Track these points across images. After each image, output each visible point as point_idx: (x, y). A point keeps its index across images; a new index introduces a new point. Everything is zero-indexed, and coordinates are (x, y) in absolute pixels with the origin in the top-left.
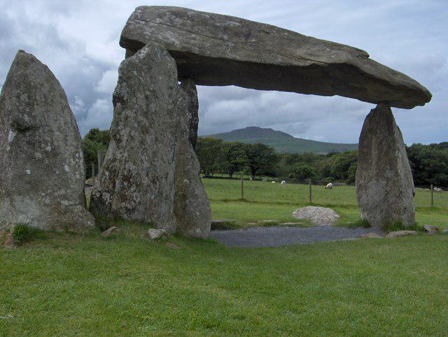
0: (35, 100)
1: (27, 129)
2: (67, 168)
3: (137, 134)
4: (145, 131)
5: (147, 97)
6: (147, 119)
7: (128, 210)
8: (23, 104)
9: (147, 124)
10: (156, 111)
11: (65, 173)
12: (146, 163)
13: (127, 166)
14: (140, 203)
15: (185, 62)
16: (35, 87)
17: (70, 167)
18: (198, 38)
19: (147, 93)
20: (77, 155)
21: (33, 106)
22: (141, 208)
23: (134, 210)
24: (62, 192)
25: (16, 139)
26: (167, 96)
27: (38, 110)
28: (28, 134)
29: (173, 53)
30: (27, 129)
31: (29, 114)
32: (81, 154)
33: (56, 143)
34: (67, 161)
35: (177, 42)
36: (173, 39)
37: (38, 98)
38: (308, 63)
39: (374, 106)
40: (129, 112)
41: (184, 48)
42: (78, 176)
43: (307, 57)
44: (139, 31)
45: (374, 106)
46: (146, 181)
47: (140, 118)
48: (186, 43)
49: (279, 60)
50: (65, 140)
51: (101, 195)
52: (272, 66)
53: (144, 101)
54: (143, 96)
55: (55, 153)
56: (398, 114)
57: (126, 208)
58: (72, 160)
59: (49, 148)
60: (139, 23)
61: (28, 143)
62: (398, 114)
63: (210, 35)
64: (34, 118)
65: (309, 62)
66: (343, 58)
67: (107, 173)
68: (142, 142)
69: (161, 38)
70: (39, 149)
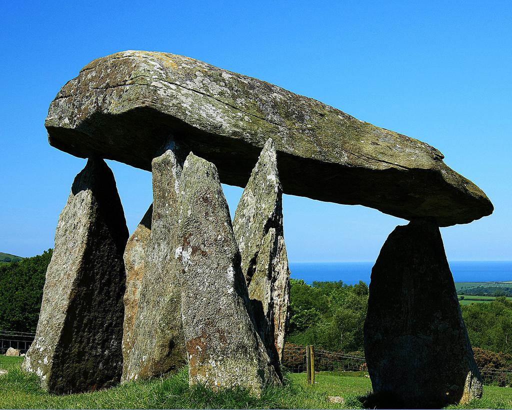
15: (218, 151)
18: (246, 118)
35: (225, 125)
36: (218, 119)
38: (383, 166)
39: (405, 222)
41: (235, 133)
43: (380, 157)
44: (175, 101)
45: (405, 222)
48: (236, 126)
49: (344, 159)
52: (336, 166)
63: (259, 115)
65: (386, 164)
66: (426, 163)
69: (205, 116)
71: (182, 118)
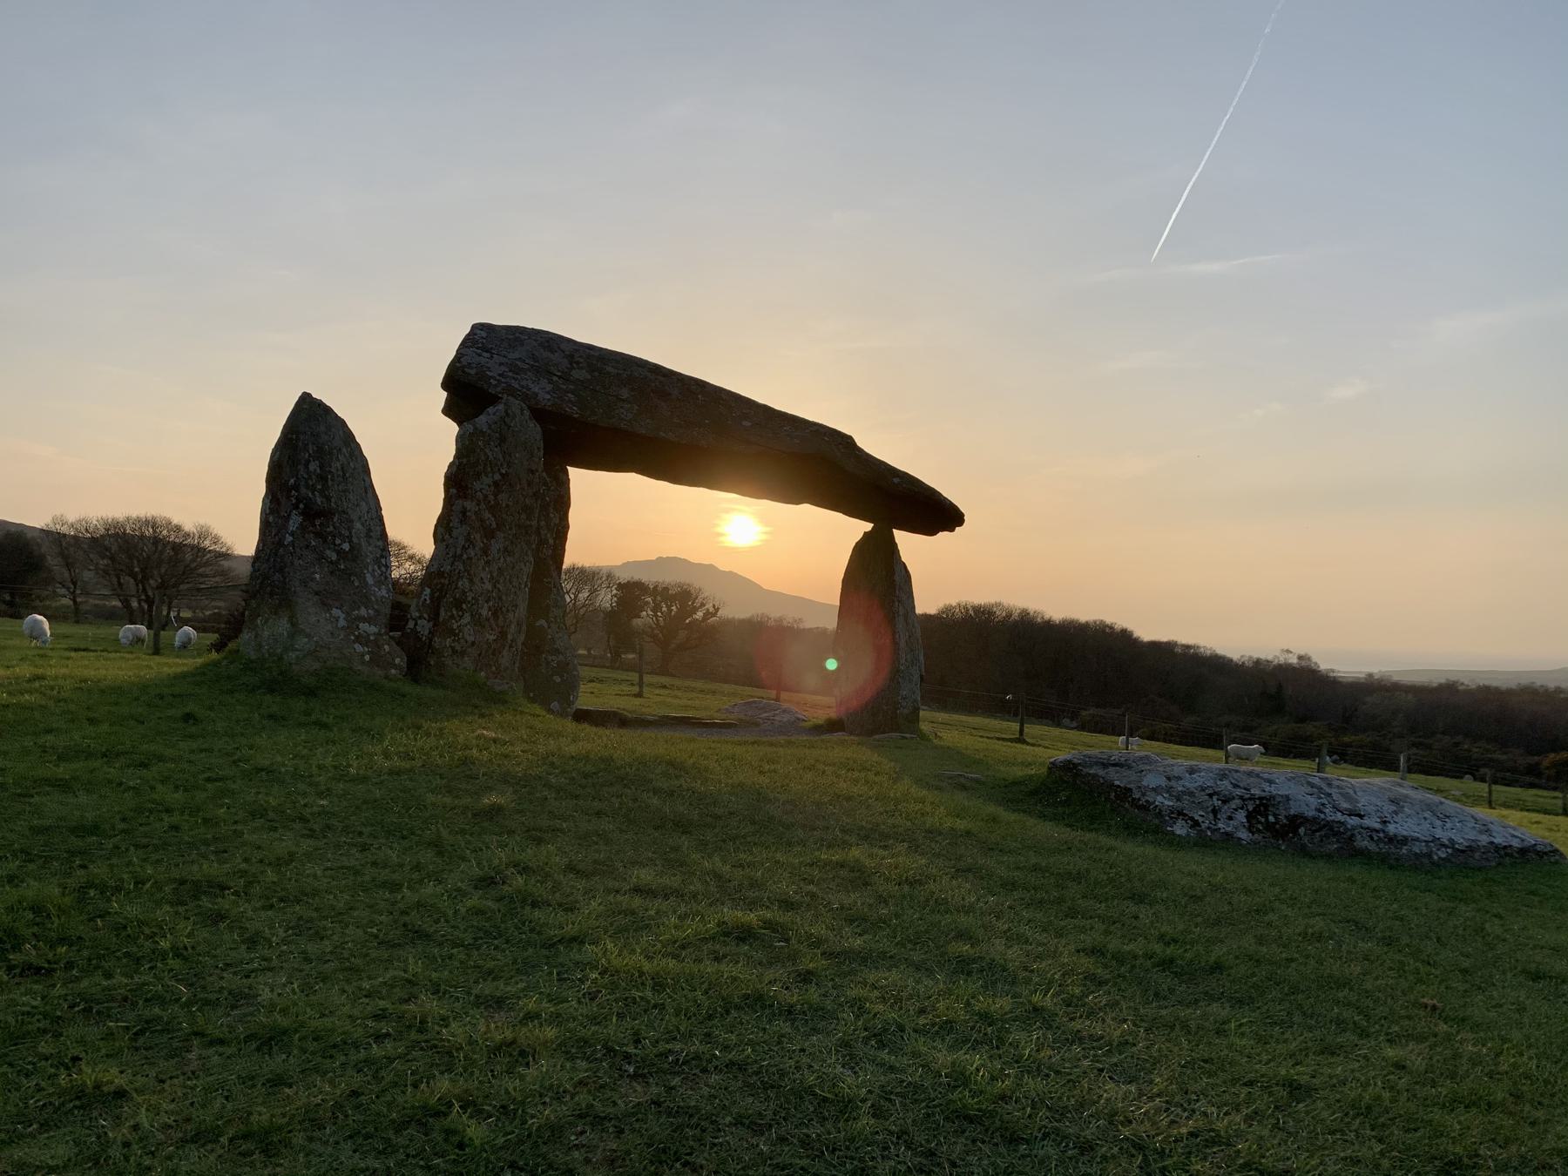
0: (330, 472)
1: (319, 514)
2: (370, 580)
3: (478, 536)
4: (490, 534)
5: (496, 484)
6: (495, 517)
7: (454, 651)
8: (314, 477)
9: (494, 526)
10: (507, 506)
12: (487, 583)
13: (460, 583)
14: (473, 643)
17: (373, 576)
19: (497, 477)
21: (327, 481)
23: (463, 653)
24: (363, 612)
25: (302, 527)
28: (317, 522)
29: (539, 414)
30: (319, 514)
31: (322, 492)
33: (355, 540)
34: (370, 569)
39: (869, 526)
40: (469, 505)
45: (869, 526)
47: (487, 515)
51: (416, 624)
53: (492, 488)
56: (908, 543)
57: (453, 648)
58: (376, 567)
59: (346, 547)
60: (480, 355)
61: (318, 535)
62: (908, 543)
64: (328, 499)
67: (428, 591)
68: (485, 551)
69: (517, 386)
70: (332, 546)
71: (485, 387)
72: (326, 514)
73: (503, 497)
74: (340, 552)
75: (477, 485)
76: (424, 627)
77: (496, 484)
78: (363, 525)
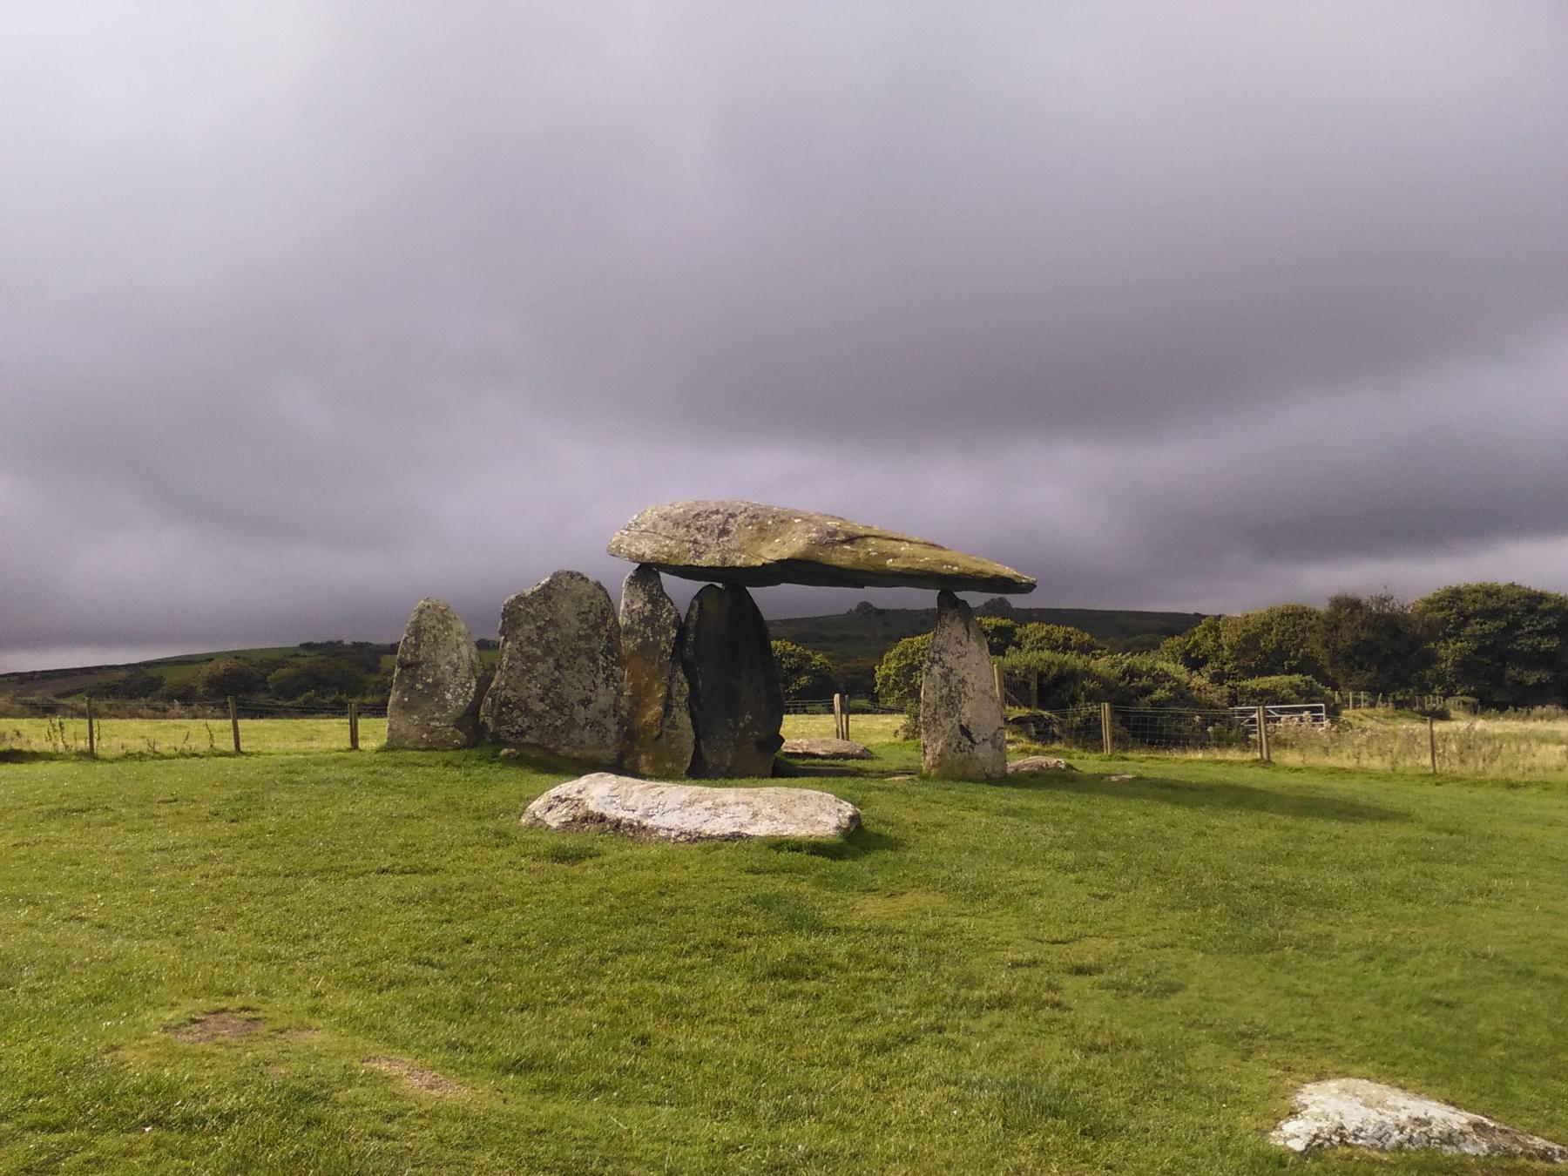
2: (449, 696)
7: (512, 734)
9: (539, 653)
11: (443, 698)
16: (425, 630)
20: (468, 685)
22: (536, 733)
23: (522, 733)
24: (437, 715)
26: (577, 623)
27: (422, 653)
28: (410, 670)
32: (474, 684)
33: (439, 676)
37: (425, 639)
42: (461, 703)
46: (539, 707)
50: (456, 671)
54: (533, 627)
55: (438, 684)
57: (508, 731)
59: (430, 680)
64: (418, 656)
68: (529, 671)
72: (420, 663)
73: (550, 635)
74: (426, 685)
75: (519, 632)
76: (490, 722)
77: (539, 628)
78: (452, 666)
